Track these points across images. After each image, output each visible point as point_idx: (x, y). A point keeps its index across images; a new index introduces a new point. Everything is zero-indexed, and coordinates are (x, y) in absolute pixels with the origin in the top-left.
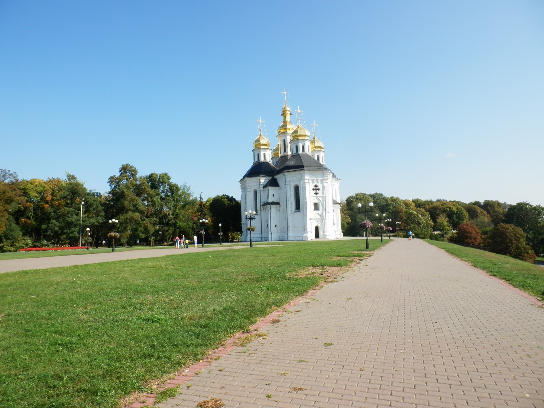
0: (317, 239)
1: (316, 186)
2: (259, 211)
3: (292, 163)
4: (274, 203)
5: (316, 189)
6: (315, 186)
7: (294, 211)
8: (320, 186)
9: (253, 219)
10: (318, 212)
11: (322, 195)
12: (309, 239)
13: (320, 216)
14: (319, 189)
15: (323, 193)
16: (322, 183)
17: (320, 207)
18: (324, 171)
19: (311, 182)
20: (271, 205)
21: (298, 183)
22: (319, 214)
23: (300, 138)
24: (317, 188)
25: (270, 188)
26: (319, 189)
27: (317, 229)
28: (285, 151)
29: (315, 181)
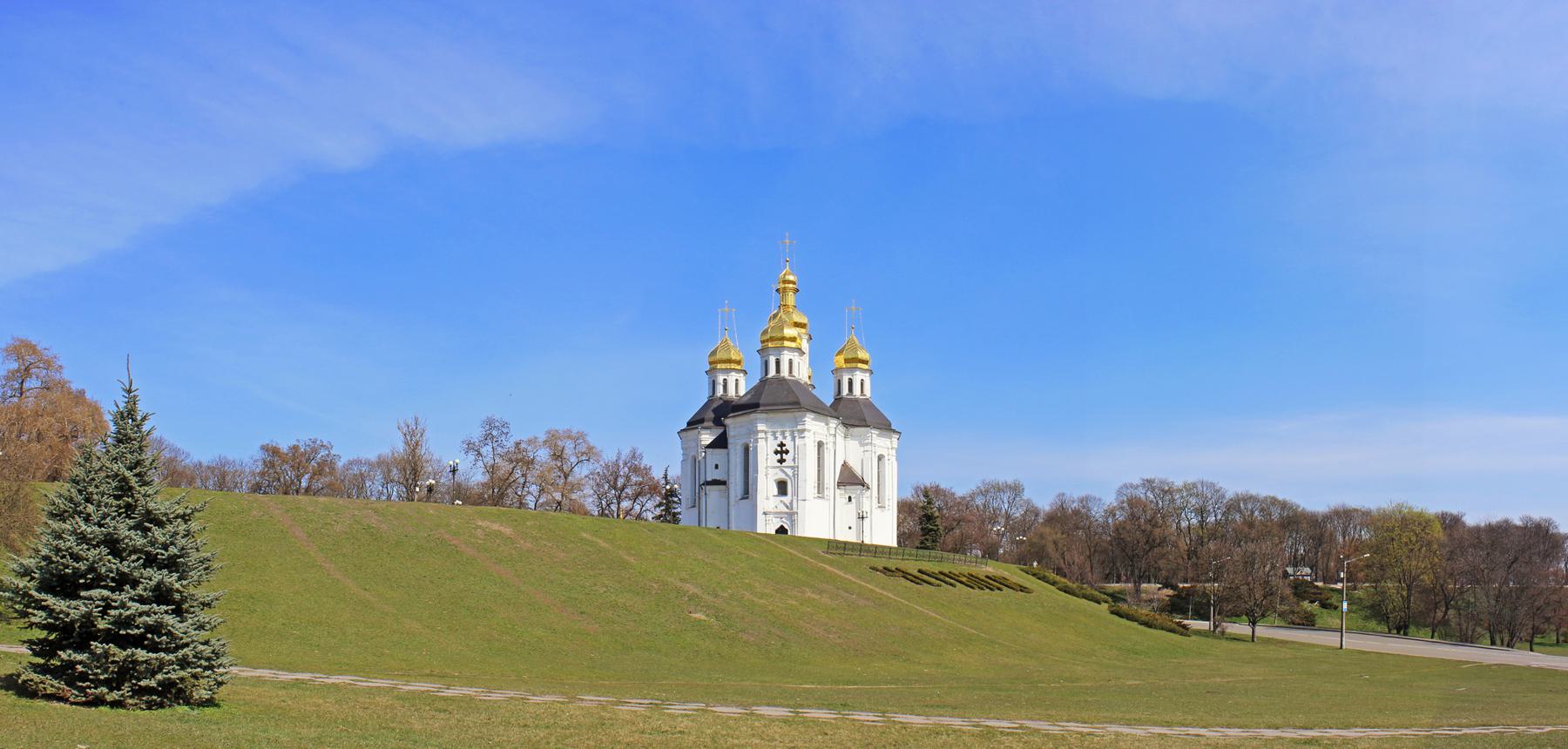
1: (782, 445)
4: (715, 482)
5: (781, 451)
6: (779, 446)
7: (740, 497)
8: (789, 445)
10: (783, 498)
11: (792, 464)
13: (787, 507)
14: (787, 452)
15: (794, 460)
16: (794, 439)
19: (770, 437)
20: (708, 487)
22: (784, 504)
24: (784, 448)
25: (709, 451)
26: (787, 452)
28: (778, 370)
29: (778, 435)
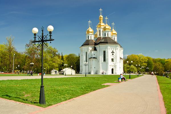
0: (113, 74)
1: (113, 51)
2: (88, 61)
3: (103, 41)
4: (94, 58)
5: (113, 52)
8: (114, 51)
9: (48, 42)
10: (113, 62)
11: (115, 55)
12: (109, 74)
17: (114, 60)
18: (117, 45)
19: (111, 50)
21: (105, 50)
23: (106, 30)
27: (112, 70)
29: (112, 49)
